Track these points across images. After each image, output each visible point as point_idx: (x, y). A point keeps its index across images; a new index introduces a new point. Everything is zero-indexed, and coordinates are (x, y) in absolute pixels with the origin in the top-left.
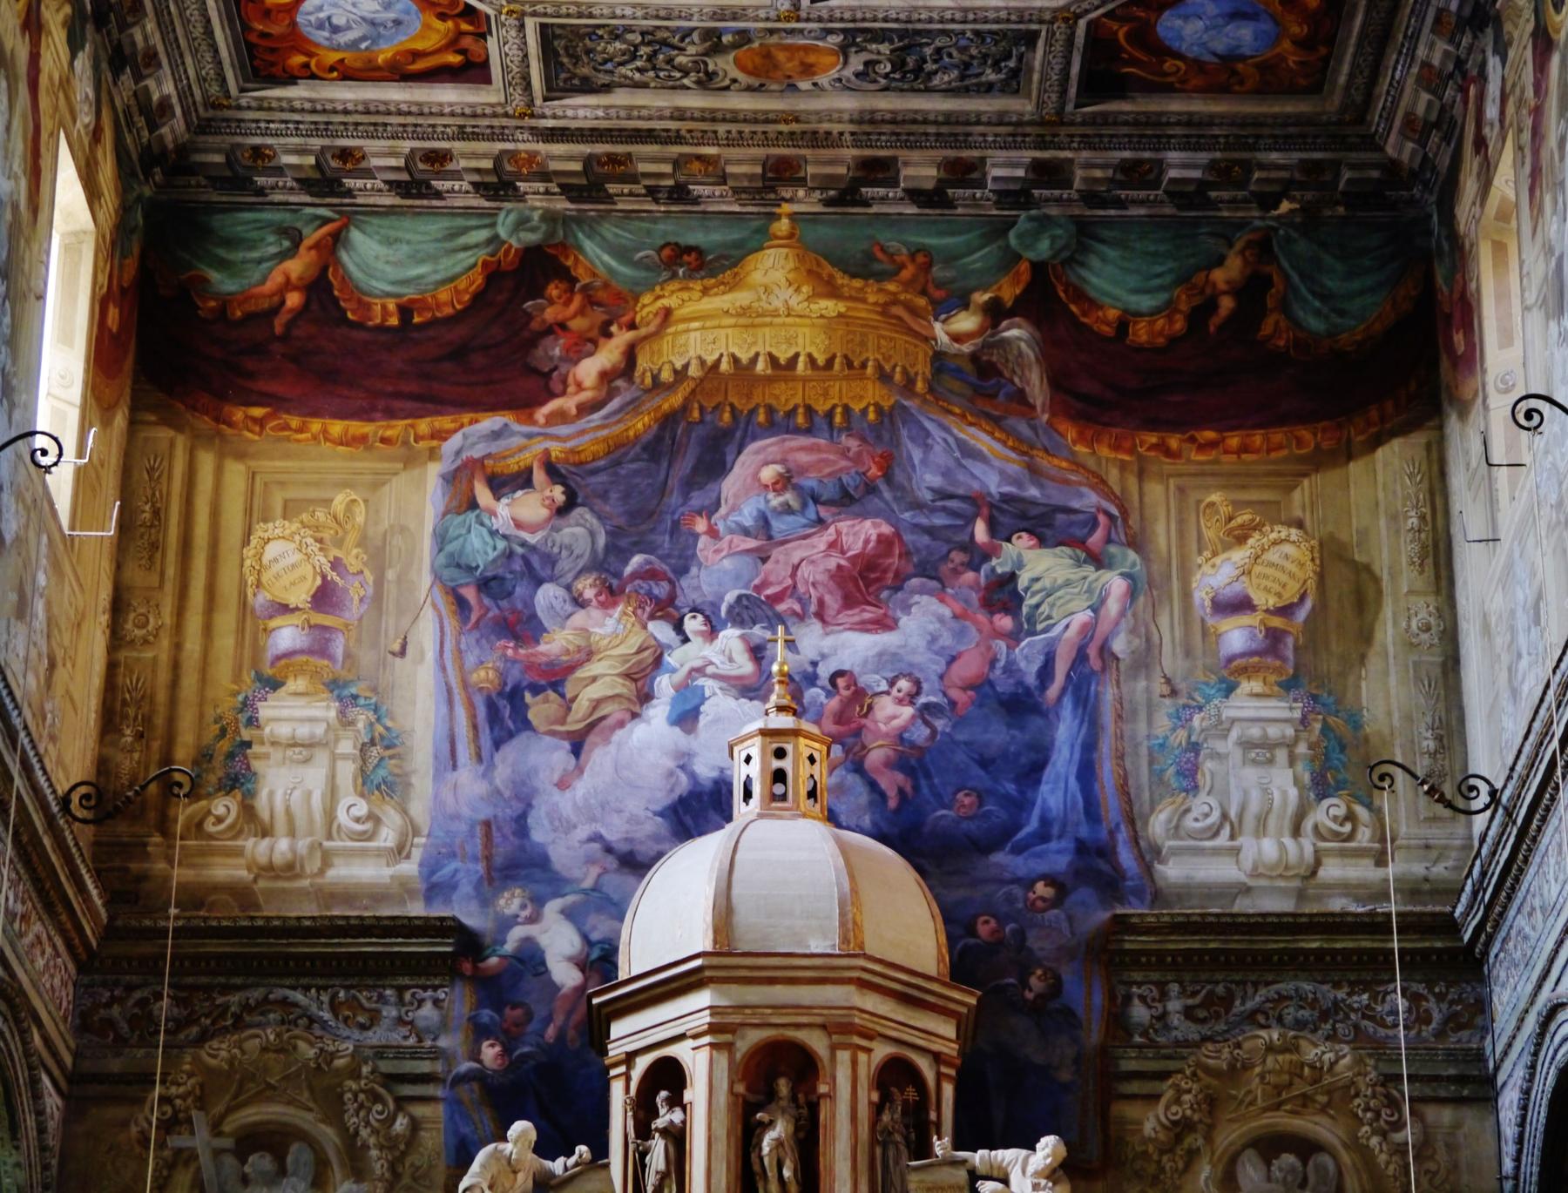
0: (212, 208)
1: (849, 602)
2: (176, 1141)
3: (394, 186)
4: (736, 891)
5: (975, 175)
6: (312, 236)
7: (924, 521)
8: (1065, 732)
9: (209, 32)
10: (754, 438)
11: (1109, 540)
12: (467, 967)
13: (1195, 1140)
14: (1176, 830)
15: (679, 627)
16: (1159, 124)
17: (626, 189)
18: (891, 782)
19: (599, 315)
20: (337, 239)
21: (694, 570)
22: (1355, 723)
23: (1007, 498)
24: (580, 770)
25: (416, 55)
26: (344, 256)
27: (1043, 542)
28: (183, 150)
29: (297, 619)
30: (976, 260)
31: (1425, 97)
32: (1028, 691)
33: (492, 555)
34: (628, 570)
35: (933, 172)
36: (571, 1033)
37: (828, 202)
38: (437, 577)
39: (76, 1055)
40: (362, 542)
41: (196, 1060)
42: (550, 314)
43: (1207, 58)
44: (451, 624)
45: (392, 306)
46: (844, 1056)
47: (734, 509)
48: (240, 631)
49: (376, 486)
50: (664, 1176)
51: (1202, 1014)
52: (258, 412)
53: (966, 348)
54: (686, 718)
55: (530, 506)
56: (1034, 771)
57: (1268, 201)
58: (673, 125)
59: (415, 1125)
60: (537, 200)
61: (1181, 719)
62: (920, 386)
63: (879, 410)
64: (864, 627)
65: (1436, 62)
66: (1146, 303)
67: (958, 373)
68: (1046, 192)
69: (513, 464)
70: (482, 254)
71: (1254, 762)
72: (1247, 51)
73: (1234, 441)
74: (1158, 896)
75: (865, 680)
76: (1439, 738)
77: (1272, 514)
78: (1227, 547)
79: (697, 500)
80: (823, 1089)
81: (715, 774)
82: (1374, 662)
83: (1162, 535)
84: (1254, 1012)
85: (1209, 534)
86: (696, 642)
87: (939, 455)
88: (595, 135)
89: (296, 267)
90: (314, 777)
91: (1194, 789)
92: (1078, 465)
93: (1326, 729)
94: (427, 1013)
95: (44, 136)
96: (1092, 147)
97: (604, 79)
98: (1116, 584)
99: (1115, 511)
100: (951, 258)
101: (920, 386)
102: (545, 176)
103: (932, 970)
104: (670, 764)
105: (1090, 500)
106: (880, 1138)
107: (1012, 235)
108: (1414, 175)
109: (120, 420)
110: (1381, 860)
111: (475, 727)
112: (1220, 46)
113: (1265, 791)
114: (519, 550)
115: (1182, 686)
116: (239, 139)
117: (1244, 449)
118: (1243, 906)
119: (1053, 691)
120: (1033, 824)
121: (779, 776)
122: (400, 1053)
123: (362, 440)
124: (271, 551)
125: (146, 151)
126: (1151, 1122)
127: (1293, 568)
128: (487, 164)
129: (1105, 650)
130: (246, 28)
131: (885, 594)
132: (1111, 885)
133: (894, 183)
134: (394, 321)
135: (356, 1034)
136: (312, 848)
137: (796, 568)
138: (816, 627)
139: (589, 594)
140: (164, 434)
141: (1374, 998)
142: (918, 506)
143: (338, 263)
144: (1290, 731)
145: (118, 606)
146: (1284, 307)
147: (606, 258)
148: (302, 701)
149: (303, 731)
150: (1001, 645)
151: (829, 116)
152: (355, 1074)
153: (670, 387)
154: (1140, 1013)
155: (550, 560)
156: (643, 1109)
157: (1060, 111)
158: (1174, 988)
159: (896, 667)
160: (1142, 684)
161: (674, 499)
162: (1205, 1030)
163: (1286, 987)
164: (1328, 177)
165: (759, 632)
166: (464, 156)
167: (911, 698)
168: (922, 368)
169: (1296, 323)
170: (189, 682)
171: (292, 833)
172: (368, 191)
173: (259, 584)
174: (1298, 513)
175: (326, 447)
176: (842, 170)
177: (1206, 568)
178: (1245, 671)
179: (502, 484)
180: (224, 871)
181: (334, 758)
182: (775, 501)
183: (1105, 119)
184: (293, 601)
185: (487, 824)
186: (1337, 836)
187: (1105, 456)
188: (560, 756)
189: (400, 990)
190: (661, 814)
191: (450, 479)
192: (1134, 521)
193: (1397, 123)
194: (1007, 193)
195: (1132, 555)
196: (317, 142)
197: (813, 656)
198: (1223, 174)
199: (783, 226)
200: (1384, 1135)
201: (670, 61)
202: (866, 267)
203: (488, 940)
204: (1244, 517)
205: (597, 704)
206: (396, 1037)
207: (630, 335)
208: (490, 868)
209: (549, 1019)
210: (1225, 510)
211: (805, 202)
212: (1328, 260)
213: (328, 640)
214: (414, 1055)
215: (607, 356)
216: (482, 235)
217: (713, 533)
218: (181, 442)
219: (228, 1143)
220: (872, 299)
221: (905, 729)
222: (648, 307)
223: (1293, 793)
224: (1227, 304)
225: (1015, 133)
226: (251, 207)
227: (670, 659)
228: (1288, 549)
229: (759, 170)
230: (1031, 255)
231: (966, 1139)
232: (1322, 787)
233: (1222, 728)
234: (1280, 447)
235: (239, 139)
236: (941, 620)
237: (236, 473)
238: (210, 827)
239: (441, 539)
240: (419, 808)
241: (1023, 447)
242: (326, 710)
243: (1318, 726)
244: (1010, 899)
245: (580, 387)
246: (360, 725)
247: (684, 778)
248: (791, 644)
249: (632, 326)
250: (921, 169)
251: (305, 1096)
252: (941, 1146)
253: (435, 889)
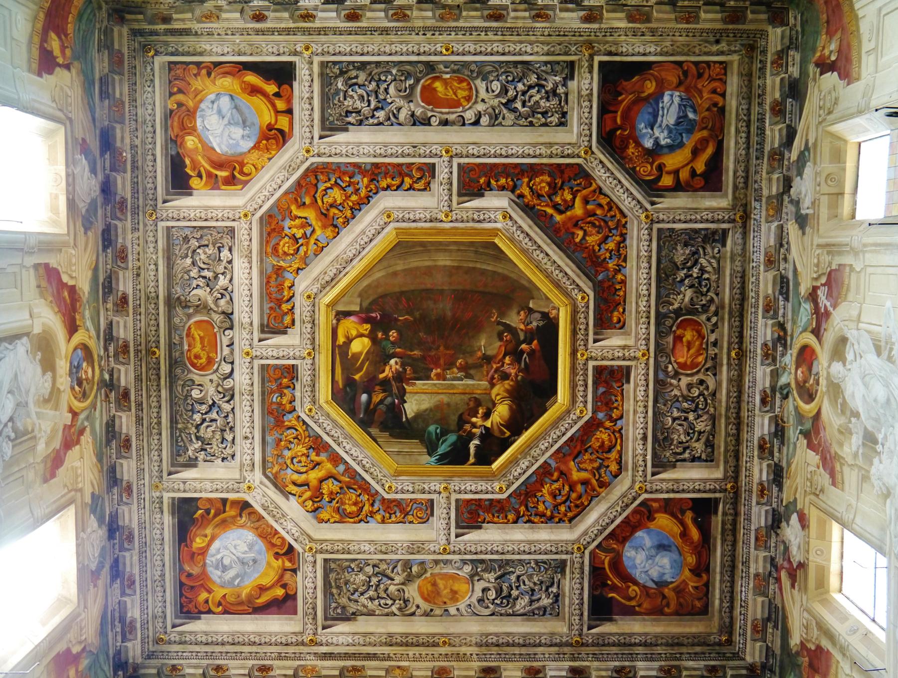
9: (163, 576)
25: (262, 589)
28: (136, 667)
31: (760, 599)
43: (651, 584)
58: (386, 650)
65: (761, 570)
72: (668, 578)
88: (347, 656)
96: (598, 660)
97: (353, 607)
108: (764, 666)
112: (654, 573)
125: (118, 653)
130: (181, 570)
164: (720, 674)
166: (279, 668)
176: (472, 673)
193: (752, 576)
201: (386, 590)
229: (430, 674)
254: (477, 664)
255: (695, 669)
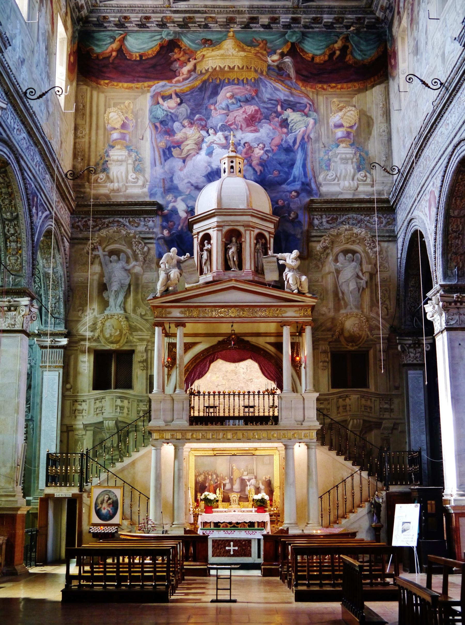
0: (94, 32)
1: (248, 126)
2: (95, 253)
3: (137, 25)
4: (222, 194)
5: (278, 21)
6: (118, 38)
7: (265, 106)
8: (299, 156)
10: (225, 86)
11: (310, 110)
12: (160, 213)
13: (328, 251)
14: (325, 179)
15: (208, 132)
16: (322, 8)
17: (193, 25)
18: (258, 168)
19: (187, 56)
20: (124, 39)
21: (211, 118)
22: (367, 154)
23: (285, 100)
24: (185, 166)
26: (126, 43)
27: (294, 111)
28: (87, 17)
29: (118, 131)
30: (278, 42)
32: (290, 147)
33: (163, 115)
34: (195, 118)
35: (267, 20)
36: (184, 228)
37: (242, 28)
38: (150, 120)
39: (71, 233)
40: (132, 112)
41: (99, 235)
42: (176, 56)
44: (154, 132)
45: (138, 55)
46: (248, 232)
47: (221, 103)
48: (104, 134)
49: (135, 99)
50: (207, 260)
51: (330, 222)
52: (107, 81)
53: (276, 64)
54: (210, 154)
55: (172, 103)
56: (292, 166)
57: (348, 27)
58: (204, 9)
59: (149, 249)
60: (172, 28)
61: (327, 153)
62: (264, 73)
63: (255, 79)
64: (251, 132)
66: (318, 52)
67: (273, 70)
68: (295, 25)
69: (167, 93)
70: (159, 42)
71: (344, 163)
73: (339, 86)
74: (321, 195)
75: (252, 144)
76: (386, 157)
77: (348, 104)
78: (337, 112)
79: (212, 101)
80: (243, 240)
81: (217, 167)
82: (371, 139)
83: (322, 109)
84: (343, 222)
85: (333, 109)
86: (212, 135)
87: (269, 90)
89: (115, 46)
90: (123, 169)
91: (329, 170)
92: (302, 92)
93: (360, 155)
94: (151, 223)
95: (54, 15)
96: (305, 14)
98: (311, 121)
99: (311, 103)
100: (272, 42)
101: (264, 73)
102: (174, 22)
103: (268, 212)
104: (206, 165)
105: (305, 101)
106: (256, 251)
107: (287, 37)
108: (383, 21)
109: (74, 84)
110: (372, 186)
111: (160, 156)
113: (346, 170)
114: (169, 114)
115: (326, 145)
116: (100, 14)
117: (342, 88)
118: (340, 197)
119: (296, 147)
120: (292, 178)
121: (232, 167)
122: (145, 233)
123: (131, 88)
124: (111, 115)
125: (78, 18)
126: (318, 247)
127: (353, 117)
128: (160, 19)
129: (309, 137)
131: (256, 124)
132: (310, 192)
133: (258, 23)
134: (138, 59)
135: (135, 228)
136: (123, 185)
137: (235, 117)
138: (240, 132)
139: (186, 124)
140: (85, 87)
141: (370, 218)
142: (264, 102)
143: (124, 44)
144: (352, 156)
145: (76, 129)
146: (352, 53)
147: (189, 42)
148: (119, 151)
149: (120, 158)
150: (284, 136)
151: (242, 6)
152: (135, 238)
153: (204, 74)
154: (316, 222)
155: (177, 116)
156: (202, 245)
157: (298, 5)
158: (324, 216)
159: (259, 141)
160: (317, 145)
161: (206, 101)
162: (331, 226)
163: (350, 216)
164: (362, 21)
165: (226, 133)
166: (154, 17)
167: (263, 149)
168: (265, 69)
169: (354, 57)
170: (93, 146)
171: (118, 182)
172: (131, 27)
173: (108, 123)
174: (354, 104)
175: (123, 90)
176: (245, 20)
177: (333, 117)
178: (342, 142)
179: (165, 98)
180: (103, 191)
181: (127, 164)
182: (230, 101)
183: (309, 7)
184: (116, 127)
185: (164, 179)
186: (362, 180)
187: (309, 90)
188: (180, 163)
189: (145, 218)
190: (204, 177)
191: (153, 97)
192: (315, 106)
193: (379, 7)
194: (285, 25)
195: (315, 114)
196: (119, 15)
197: (239, 138)
198: (338, 20)
199: (231, 34)
200: (372, 249)
202: (251, 44)
203: (164, 206)
204: (341, 105)
205: (189, 150)
206: (144, 229)
207: (195, 61)
208: (164, 190)
209: (179, 225)
210: (337, 103)
211: (236, 28)
212: (362, 42)
213: (125, 136)
214: (148, 233)
215: (189, 66)
216: (159, 37)
217: (215, 109)
218: (89, 89)
219: (107, 253)
220: (253, 52)
221: (262, 156)
222: (199, 55)
223: (352, 170)
224: (338, 53)
225: (287, 10)
226: (103, 31)
227: (206, 140)
228: (352, 112)
229: (225, 20)
230: (291, 41)
231: (276, 251)
232: (359, 169)
233: (336, 155)
234: (350, 88)
235: (100, 14)
236: (270, 130)
237: (102, 96)
238: (99, 181)
239: (151, 111)
240: (147, 176)
241: (289, 88)
242: (125, 153)
243: (358, 155)
244: (286, 196)
245: (183, 74)
246: (133, 156)
247: (209, 168)
248: (234, 136)
249: (195, 59)
250: (264, 19)
251: (124, 243)
252: (270, 252)
253: (151, 195)
254: (247, 16)
255: (351, 19)
